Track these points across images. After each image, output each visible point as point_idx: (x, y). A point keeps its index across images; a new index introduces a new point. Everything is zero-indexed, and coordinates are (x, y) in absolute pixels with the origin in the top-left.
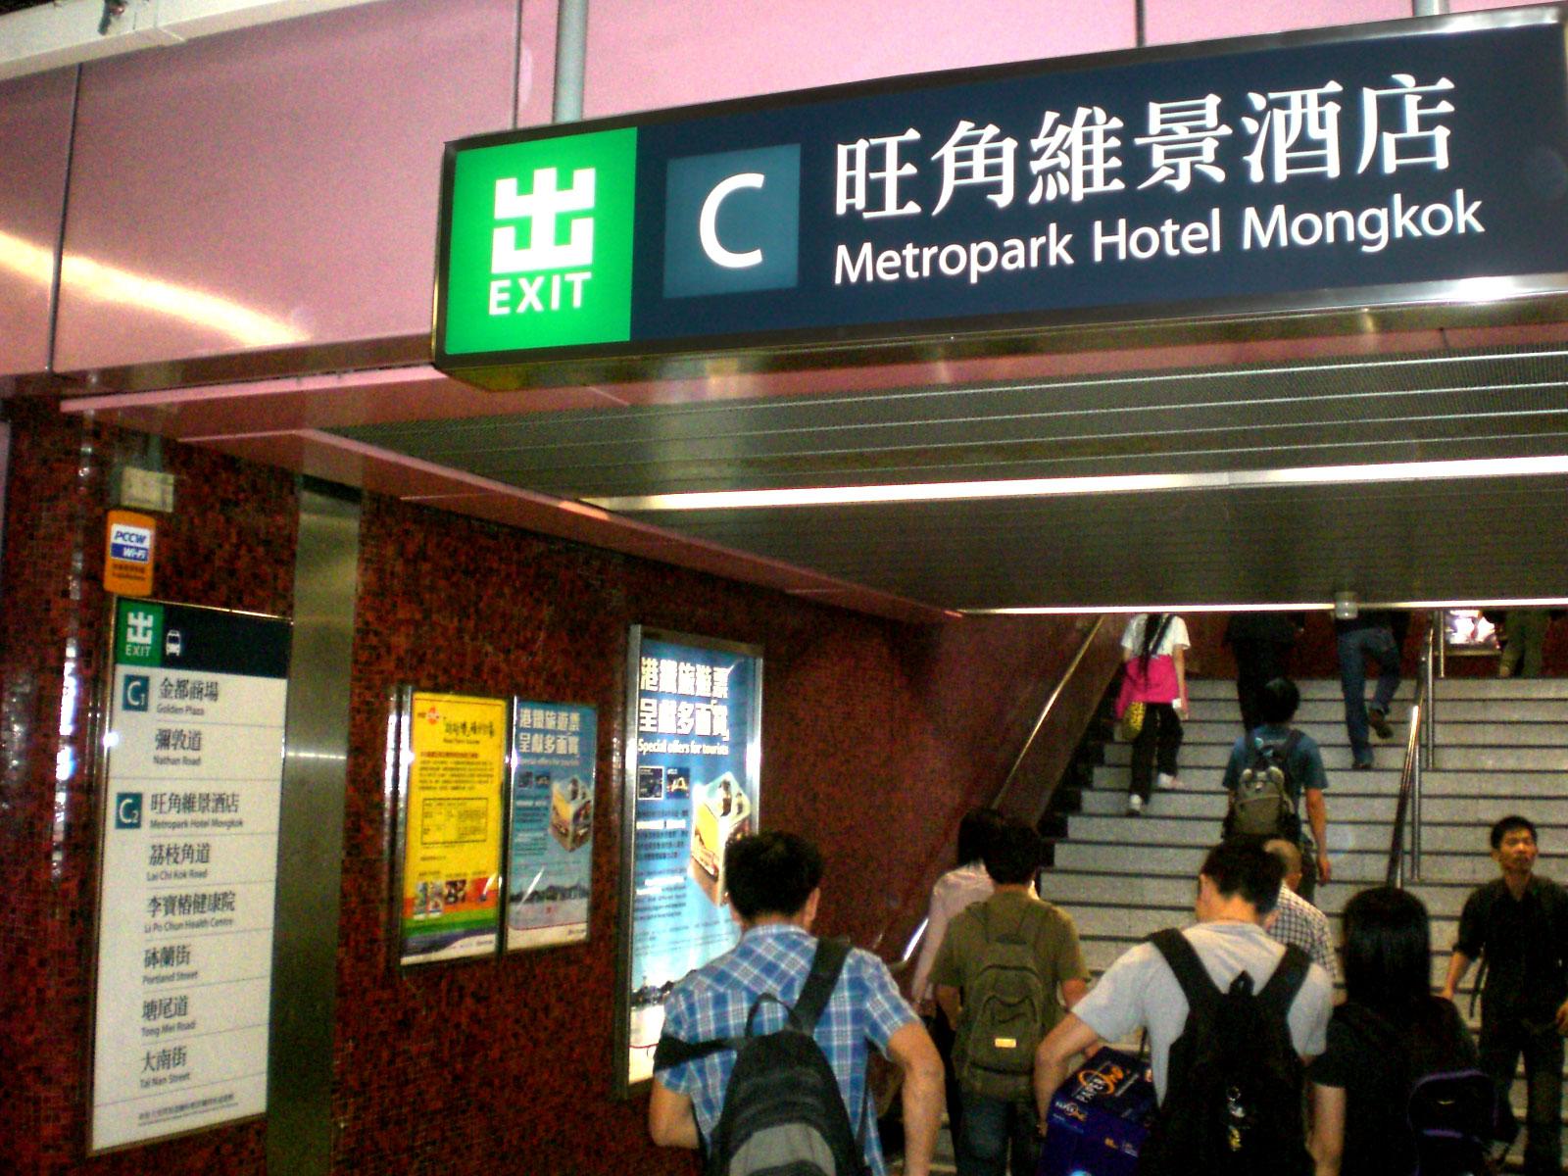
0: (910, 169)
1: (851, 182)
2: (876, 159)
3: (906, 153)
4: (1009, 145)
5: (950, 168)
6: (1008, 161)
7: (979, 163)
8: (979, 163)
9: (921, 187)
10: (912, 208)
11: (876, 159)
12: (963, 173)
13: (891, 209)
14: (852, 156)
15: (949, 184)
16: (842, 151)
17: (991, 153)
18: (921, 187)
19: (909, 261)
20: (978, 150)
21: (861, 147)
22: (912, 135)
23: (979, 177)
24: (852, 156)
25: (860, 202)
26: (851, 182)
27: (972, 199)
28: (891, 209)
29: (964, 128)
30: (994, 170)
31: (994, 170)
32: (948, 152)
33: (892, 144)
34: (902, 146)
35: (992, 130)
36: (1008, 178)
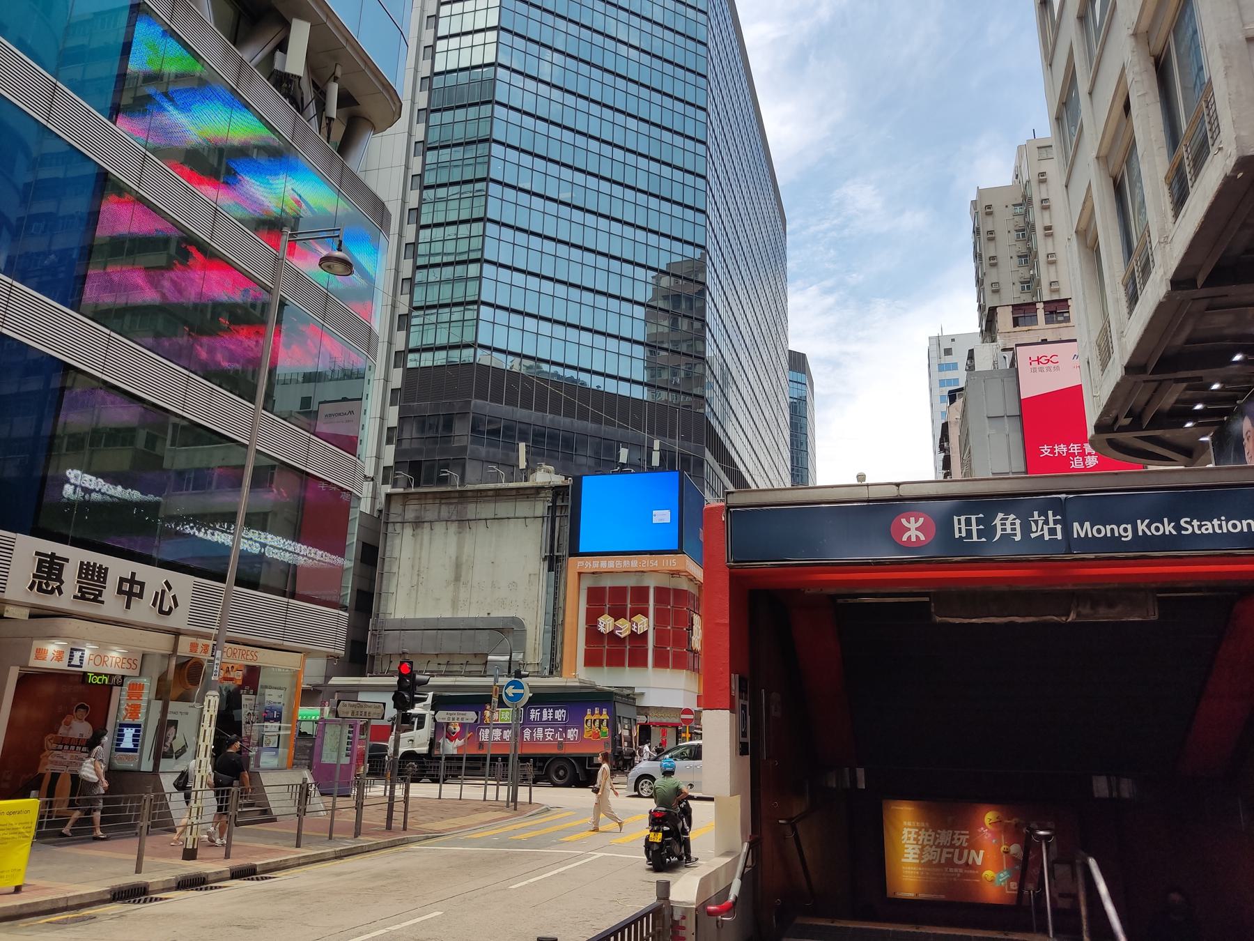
2: (968, 522)
3: (979, 522)
4: (1018, 522)
5: (999, 528)
6: (1018, 527)
7: (1008, 527)
8: (1008, 527)
11: (968, 522)
13: (975, 539)
16: (956, 518)
20: (1008, 523)
21: (963, 518)
23: (1009, 531)
25: (964, 534)
28: (975, 539)
29: (1000, 515)
30: (1014, 529)
31: (1014, 529)
32: (997, 522)
33: (973, 518)
35: (1012, 516)
36: (1018, 532)
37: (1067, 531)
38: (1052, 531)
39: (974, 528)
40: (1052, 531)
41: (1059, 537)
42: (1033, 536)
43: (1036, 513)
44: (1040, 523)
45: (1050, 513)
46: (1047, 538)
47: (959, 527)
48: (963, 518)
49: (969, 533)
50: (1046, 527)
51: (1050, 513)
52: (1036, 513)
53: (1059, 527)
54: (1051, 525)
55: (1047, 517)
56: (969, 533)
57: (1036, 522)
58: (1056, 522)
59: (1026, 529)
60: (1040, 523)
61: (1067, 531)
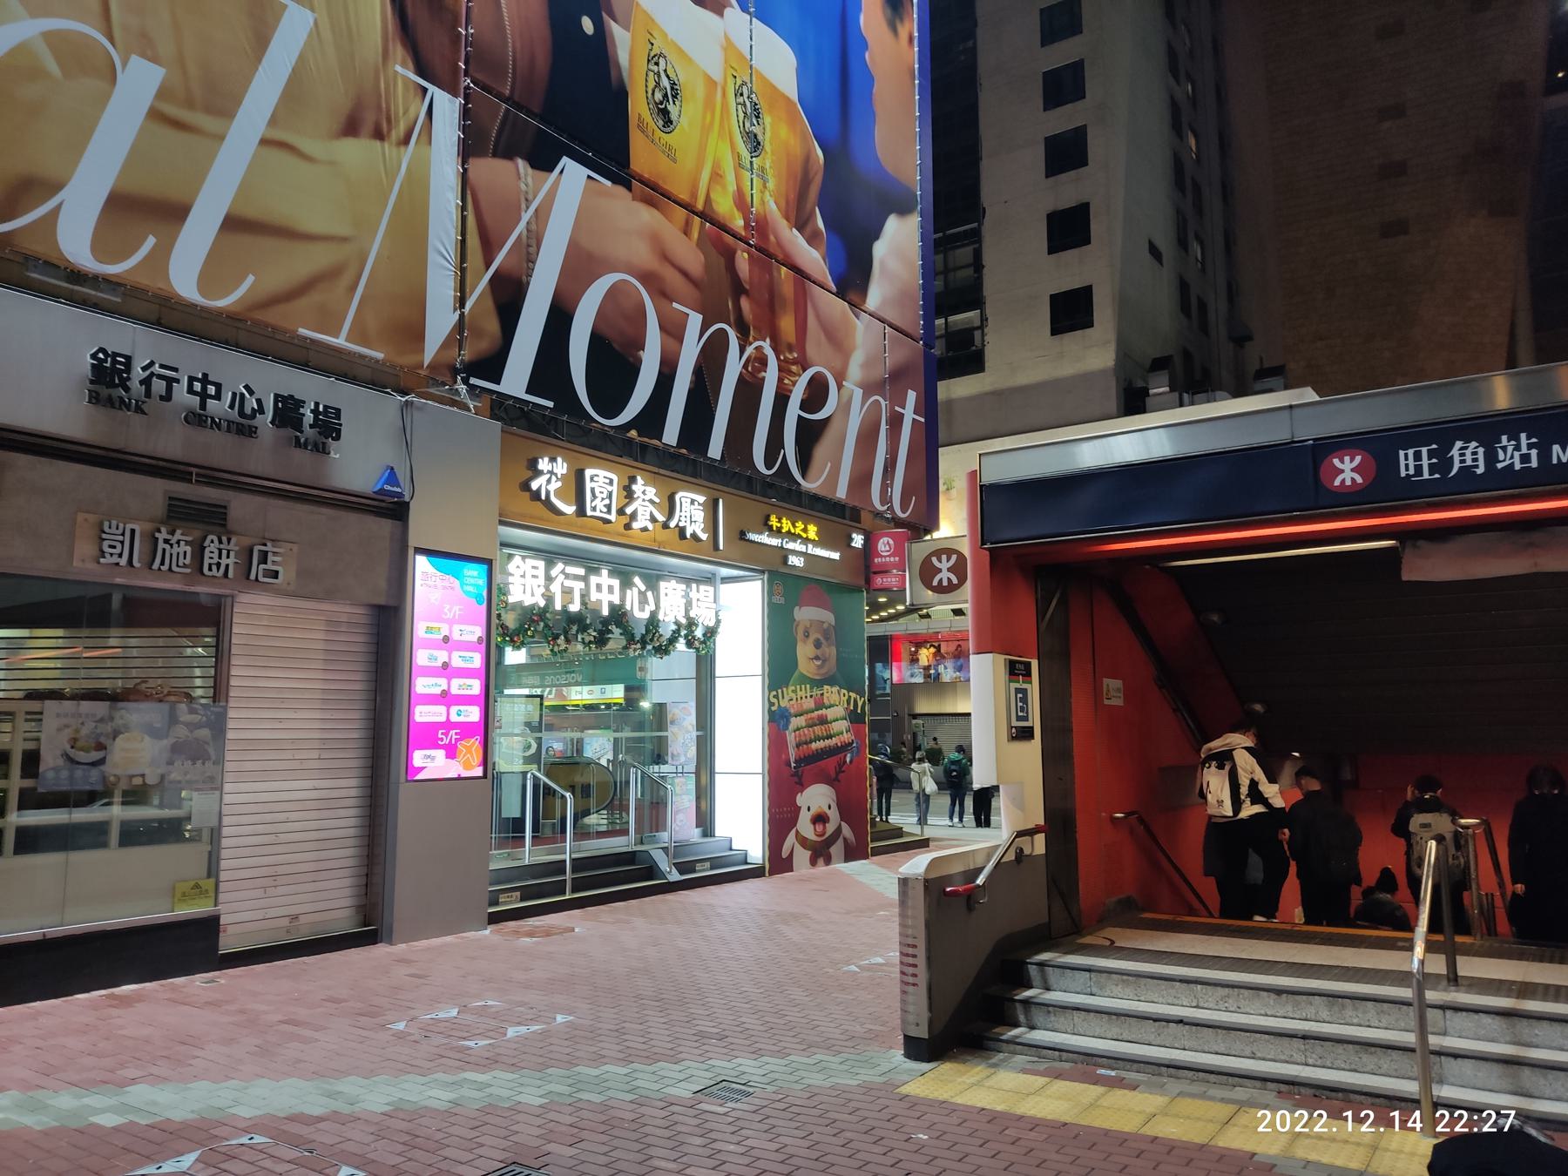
2: (1418, 456)
3: (1431, 454)
4: (1481, 450)
5: (1457, 460)
6: (1481, 456)
11: (1418, 456)
12: (1463, 461)
13: (1426, 476)
16: (1402, 453)
17: (1474, 453)
20: (1468, 452)
21: (1411, 452)
23: (1469, 463)
25: (1412, 472)
28: (1426, 476)
29: (1459, 444)
30: (1475, 460)
31: (1475, 460)
32: (1455, 452)
33: (1424, 450)
35: (1474, 444)
36: (1481, 463)
37: (1545, 455)
38: (1525, 458)
39: (1425, 462)
40: (1525, 458)
41: (1534, 464)
42: (1500, 466)
43: (1504, 438)
44: (1510, 449)
45: (1523, 436)
46: (1518, 466)
47: (1406, 462)
48: (1411, 452)
49: (1419, 469)
50: (1517, 454)
51: (1523, 436)
52: (1504, 438)
53: (1534, 452)
54: (1524, 450)
55: (1518, 440)
56: (1419, 469)
57: (1504, 449)
58: (1530, 446)
59: (1491, 458)
60: (1510, 449)
61: (1545, 455)
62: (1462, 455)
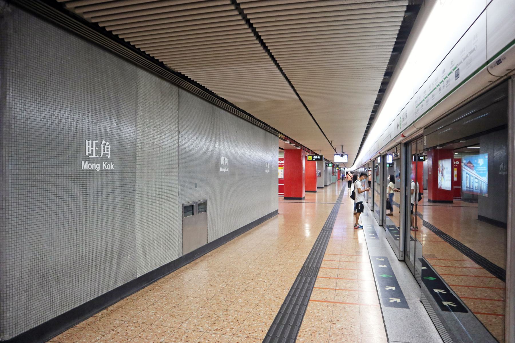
0: (97, 149)
1: (89, 148)
4: (109, 147)
5: (102, 149)
6: (109, 149)
7: (106, 149)
8: (106, 149)
9: (98, 152)
10: (98, 156)
12: (104, 151)
14: (89, 143)
15: (102, 152)
17: (108, 148)
18: (98, 152)
19: (97, 167)
20: (106, 146)
22: (97, 141)
23: (106, 152)
24: (89, 143)
25: (90, 152)
26: (89, 148)
27: (105, 155)
30: (108, 151)
31: (108, 151)
33: (94, 142)
34: (96, 143)
35: (107, 143)
36: (109, 153)
39: (94, 149)
48: (90, 142)
49: (92, 151)
56: (92, 151)
62: (104, 147)
